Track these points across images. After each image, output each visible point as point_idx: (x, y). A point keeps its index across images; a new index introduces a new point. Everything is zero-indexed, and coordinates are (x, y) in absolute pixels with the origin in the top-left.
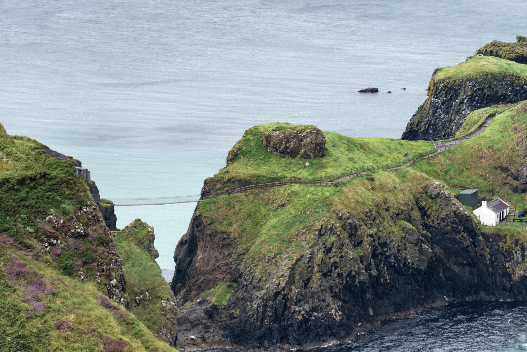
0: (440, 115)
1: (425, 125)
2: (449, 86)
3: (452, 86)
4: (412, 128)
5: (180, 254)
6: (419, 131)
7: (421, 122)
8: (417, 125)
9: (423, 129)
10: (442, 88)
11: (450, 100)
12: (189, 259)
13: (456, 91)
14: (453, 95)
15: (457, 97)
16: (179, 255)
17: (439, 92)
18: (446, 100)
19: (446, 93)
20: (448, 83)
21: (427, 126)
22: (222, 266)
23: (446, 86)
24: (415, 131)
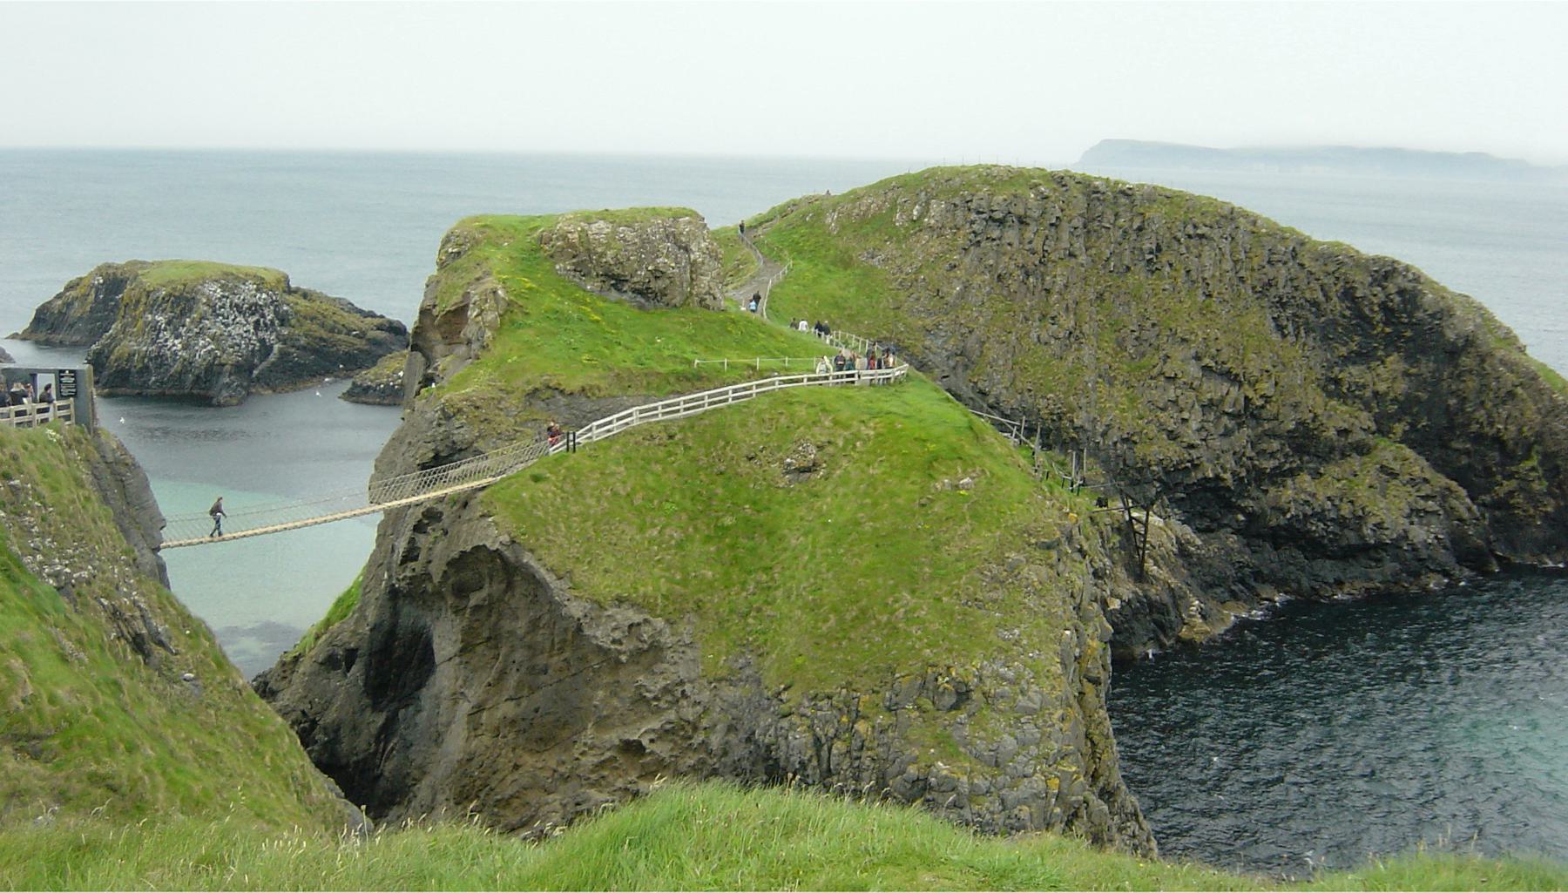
0: (166, 341)
1: (143, 358)
2: (177, 294)
3: (182, 294)
4: (118, 365)
5: (329, 703)
6: (133, 370)
7: (134, 355)
8: (127, 360)
9: (140, 365)
10: (163, 298)
11: (183, 314)
12: (380, 719)
13: (188, 300)
14: (184, 308)
15: (191, 310)
16: (325, 708)
17: (160, 306)
18: (173, 317)
19: (172, 307)
20: (174, 289)
21: (146, 360)
22: (652, 741)
23: (170, 295)
24: (123, 370)
